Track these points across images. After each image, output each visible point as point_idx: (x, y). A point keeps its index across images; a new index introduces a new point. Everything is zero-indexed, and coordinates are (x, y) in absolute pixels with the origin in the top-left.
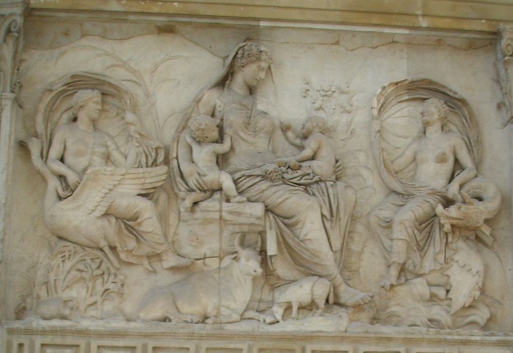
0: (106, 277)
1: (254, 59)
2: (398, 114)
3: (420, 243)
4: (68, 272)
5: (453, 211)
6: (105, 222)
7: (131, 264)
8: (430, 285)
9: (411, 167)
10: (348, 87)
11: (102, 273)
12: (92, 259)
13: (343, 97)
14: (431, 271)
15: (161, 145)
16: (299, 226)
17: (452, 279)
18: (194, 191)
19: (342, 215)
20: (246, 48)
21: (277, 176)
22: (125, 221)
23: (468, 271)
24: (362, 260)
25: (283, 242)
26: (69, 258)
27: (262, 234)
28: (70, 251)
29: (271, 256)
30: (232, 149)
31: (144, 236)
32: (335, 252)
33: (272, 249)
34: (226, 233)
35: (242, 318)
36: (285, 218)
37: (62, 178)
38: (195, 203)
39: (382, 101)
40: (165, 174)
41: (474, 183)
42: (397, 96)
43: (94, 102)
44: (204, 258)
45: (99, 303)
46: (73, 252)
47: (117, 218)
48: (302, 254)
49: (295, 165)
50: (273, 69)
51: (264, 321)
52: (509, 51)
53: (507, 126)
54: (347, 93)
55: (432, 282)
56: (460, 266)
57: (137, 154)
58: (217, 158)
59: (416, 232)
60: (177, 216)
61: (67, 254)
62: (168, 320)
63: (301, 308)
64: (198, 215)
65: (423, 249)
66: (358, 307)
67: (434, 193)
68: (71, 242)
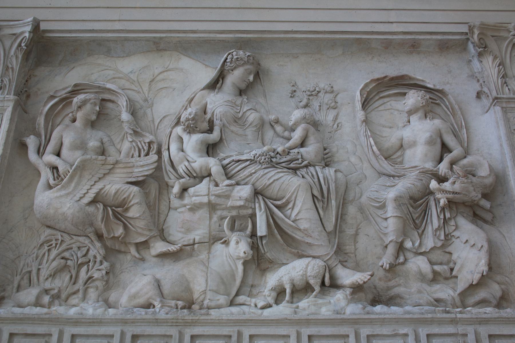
0: (91, 264)
1: (242, 62)
2: (381, 108)
3: (417, 222)
4: (54, 260)
5: (447, 185)
6: (91, 209)
7: (119, 252)
8: (432, 263)
9: (399, 154)
10: (332, 87)
11: (88, 260)
12: (79, 248)
13: (328, 95)
14: (432, 249)
15: (154, 140)
16: (290, 206)
17: (454, 257)
18: (183, 178)
19: (333, 196)
20: (234, 53)
21: (265, 159)
22: (114, 208)
23: (472, 246)
24: (357, 242)
25: (274, 224)
26: (56, 247)
27: (253, 216)
28: (56, 240)
29: (261, 237)
30: (221, 140)
31: (132, 222)
32: (329, 233)
33: (262, 230)
34: (215, 218)
35: (232, 304)
36: (275, 200)
37: (54, 168)
38: (184, 190)
39: (365, 96)
40: (156, 162)
41: (465, 161)
42: (378, 93)
43: (91, 104)
44: (194, 244)
45: (81, 292)
46: (60, 241)
47: (105, 206)
48: (294, 235)
49: (284, 151)
50: (261, 76)
51: (256, 306)
52: (482, 44)
53: (491, 111)
54: (332, 92)
55: (434, 260)
56: (462, 242)
57: (131, 148)
58: (208, 149)
59: (411, 209)
60: (167, 204)
61: (54, 242)
62: (152, 306)
63: (295, 291)
64: (187, 201)
65: (420, 227)
66: (357, 289)
67: (424, 172)
68: (60, 231)
